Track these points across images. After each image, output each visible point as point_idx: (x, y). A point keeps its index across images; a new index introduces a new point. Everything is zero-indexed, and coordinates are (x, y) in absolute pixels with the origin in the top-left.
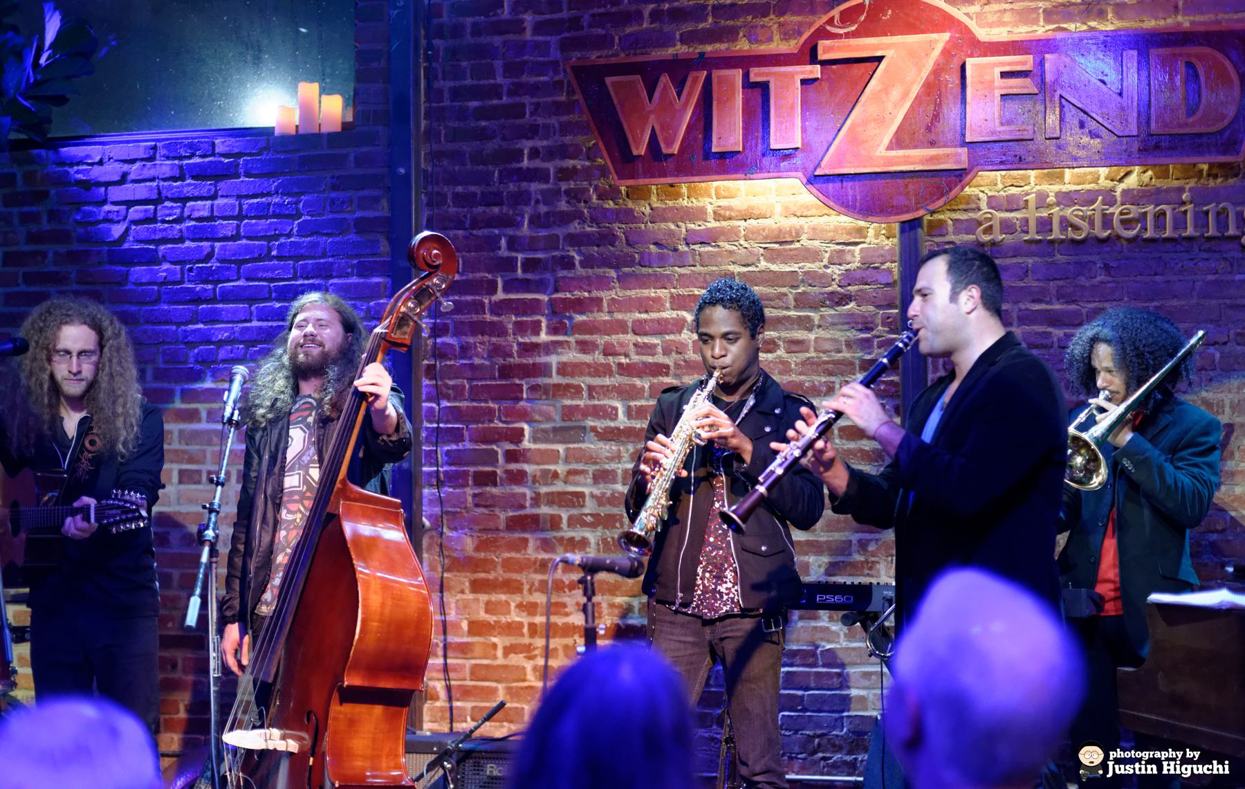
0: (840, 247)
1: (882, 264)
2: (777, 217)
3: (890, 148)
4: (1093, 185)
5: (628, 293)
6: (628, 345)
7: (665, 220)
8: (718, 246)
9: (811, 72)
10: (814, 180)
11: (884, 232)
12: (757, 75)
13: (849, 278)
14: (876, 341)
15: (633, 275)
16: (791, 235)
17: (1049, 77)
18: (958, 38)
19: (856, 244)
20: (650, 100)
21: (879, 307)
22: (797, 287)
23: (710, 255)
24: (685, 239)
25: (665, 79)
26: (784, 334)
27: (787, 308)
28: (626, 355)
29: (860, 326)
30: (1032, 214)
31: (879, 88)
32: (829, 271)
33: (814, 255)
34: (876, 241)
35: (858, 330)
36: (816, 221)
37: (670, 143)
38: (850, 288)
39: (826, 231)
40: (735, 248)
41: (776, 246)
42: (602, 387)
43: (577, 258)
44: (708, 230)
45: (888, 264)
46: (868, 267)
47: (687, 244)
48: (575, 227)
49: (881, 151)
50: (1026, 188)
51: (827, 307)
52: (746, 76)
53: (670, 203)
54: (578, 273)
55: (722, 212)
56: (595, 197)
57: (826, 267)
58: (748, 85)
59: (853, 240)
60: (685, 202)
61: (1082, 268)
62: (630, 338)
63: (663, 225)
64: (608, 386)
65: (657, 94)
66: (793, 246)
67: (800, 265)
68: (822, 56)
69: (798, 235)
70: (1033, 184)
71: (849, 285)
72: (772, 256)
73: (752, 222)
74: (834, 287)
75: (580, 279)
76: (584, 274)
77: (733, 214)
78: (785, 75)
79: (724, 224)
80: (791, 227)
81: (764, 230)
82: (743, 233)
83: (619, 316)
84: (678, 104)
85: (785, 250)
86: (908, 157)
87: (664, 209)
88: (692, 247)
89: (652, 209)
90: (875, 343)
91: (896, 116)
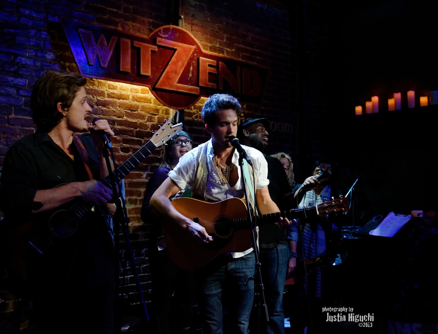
3: (178, 83)
8: (109, 108)
9: (155, 48)
10: (154, 90)
11: (164, 112)
12: (137, 44)
16: (135, 108)
17: (220, 70)
18: (197, 49)
19: (156, 115)
22: (136, 128)
23: (108, 111)
24: (96, 103)
26: (132, 146)
27: (133, 136)
31: (175, 60)
32: (147, 123)
33: (142, 117)
34: (162, 115)
36: (143, 104)
39: (147, 108)
40: (115, 110)
41: (129, 111)
44: (105, 101)
47: (97, 105)
49: (175, 83)
53: (91, 87)
55: (111, 95)
57: (146, 122)
58: (133, 47)
59: (155, 113)
60: (97, 87)
66: (135, 112)
67: (138, 120)
68: (159, 44)
72: (128, 115)
73: (121, 100)
74: (149, 130)
77: (115, 96)
79: (111, 99)
80: (135, 105)
81: (126, 104)
82: (118, 104)
85: (133, 113)
88: (100, 107)
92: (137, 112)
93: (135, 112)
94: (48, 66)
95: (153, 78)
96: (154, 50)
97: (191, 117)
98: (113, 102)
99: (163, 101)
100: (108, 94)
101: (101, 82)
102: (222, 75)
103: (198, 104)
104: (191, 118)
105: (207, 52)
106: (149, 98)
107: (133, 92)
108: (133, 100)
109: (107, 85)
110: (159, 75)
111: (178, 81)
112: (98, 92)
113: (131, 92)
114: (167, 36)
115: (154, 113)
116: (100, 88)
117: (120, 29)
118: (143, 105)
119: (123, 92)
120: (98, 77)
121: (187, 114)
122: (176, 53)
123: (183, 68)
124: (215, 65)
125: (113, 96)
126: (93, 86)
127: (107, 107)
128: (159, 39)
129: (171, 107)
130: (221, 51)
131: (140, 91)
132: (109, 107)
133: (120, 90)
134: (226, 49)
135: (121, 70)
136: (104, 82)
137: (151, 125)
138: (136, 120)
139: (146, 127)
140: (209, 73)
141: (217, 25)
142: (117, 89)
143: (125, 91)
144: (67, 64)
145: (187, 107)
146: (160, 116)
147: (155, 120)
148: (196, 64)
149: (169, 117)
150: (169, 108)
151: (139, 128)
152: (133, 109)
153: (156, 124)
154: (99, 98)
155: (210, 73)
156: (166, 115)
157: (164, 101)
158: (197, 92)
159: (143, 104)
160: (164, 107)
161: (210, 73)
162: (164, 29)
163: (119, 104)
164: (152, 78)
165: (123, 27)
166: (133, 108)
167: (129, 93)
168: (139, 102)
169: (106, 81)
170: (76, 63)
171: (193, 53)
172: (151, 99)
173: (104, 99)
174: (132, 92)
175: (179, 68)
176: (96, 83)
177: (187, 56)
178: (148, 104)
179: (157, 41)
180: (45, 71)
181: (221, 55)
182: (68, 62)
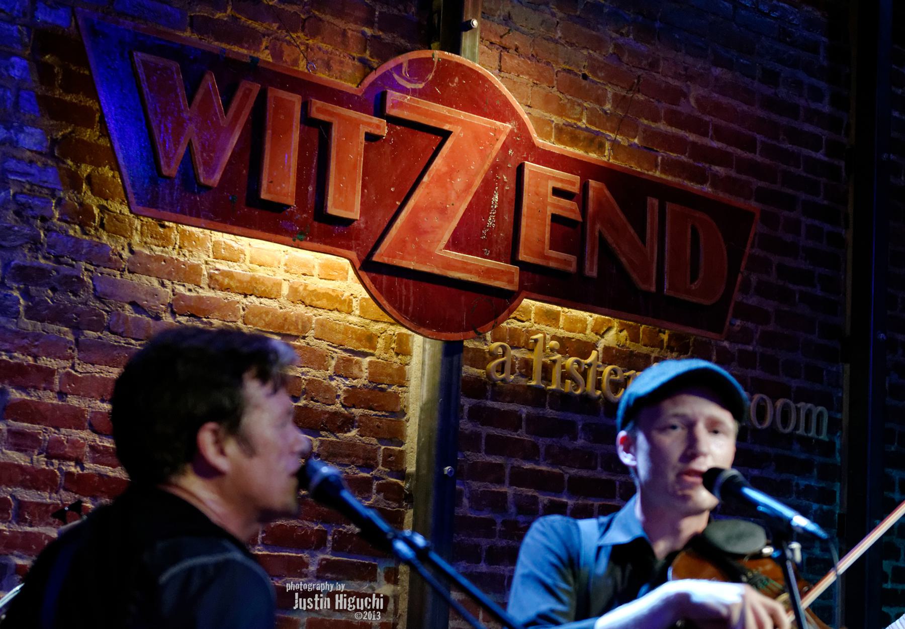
0: (346, 355)
1: (390, 385)
2: (282, 300)
3: (447, 247)
4: (581, 335)
5: (89, 368)
6: (83, 445)
7: (148, 272)
9: (378, 127)
11: (393, 345)
12: (320, 109)
13: (354, 397)
14: (375, 484)
15: (101, 345)
18: (517, 135)
19: (365, 355)
20: (191, 99)
21: (381, 440)
24: (170, 305)
25: (210, 80)
28: (79, 463)
29: (361, 462)
30: (537, 359)
31: (444, 169)
32: (334, 383)
34: (385, 356)
35: (358, 467)
36: (324, 315)
37: (210, 172)
38: (353, 410)
42: (39, 505)
43: (21, 301)
44: (200, 299)
45: (394, 388)
46: (375, 387)
47: (173, 314)
48: (23, 257)
49: (440, 250)
50: (527, 324)
51: (327, 431)
52: (305, 107)
53: (158, 250)
54: (23, 326)
55: (220, 278)
56: (57, 215)
58: (307, 121)
60: (175, 252)
61: (568, 428)
62: (85, 435)
63: (144, 278)
64: (48, 505)
65: (198, 97)
66: (297, 343)
67: (304, 369)
69: (305, 329)
70: (533, 321)
71: (354, 407)
73: (253, 299)
74: (337, 407)
75: (21, 334)
76: (30, 328)
78: (350, 119)
79: (220, 294)
80: (298, 317)
81: (267, 313)
82: (242, 313)
83: (73, 401)
84: (224, 122)
86: (466, 263)
87: (149, 257)
89: (132, 251)
90: (374, 487)
91: (458, 210)
92: (302, 341)
93: (297, 343)
94: (24, 174)
95: (366, 228)
96: (377, 132)
97: (484, 368)
98: (226, 304)
99: (395, 308)
100: (211, 276)
101: (191, 234)
102: (598, 226)
103: (507, 323)
104: (483, 371)
105: (547, 143)
106: (347, 294)
107: (292, 271)
108: (291, 299)
109: (210, 245)
110: (387, 219)
111: (449, 241)
112: (178, 269)
113: (287, 272)
114: (421, 86)
115: (359, 348)
116: (187, 254)
117: (265, 56)
118: (323, 320)
119: (261, 273)
120: (182, 217)
121: (470, 354)
122: (449, 144)
123: (470, 198)
124: (575, 189)
125: (228, 284)
126: (164, 247)
127: (205, 320)
128: (393, 96)
129: (422, 330)
130: (594, 141)
131: (316, 272)
132: (212, 321)
133: (251, 263)
134: (613, 135)
135: (264, 196)
136: (201, 235)
137: (345, 388)
138: (299, 369)
139: (329, 394)
140: (553, 216)
141: (585, 52)
142: (241, 260)
143: (269, 268)
144: (86, 170)
145: (472, 333)
146: (379, 359)
147: (362, 371)
148: (513, 185)
149: (407, 364)
150: (410, 332)
151: (305, 399)
152: (289, 330)
153: (364, 385)
154: (181, 289)
155: (555, 218)
156: (400, 357)
157: (399, 310)
158: (510, 282)
159: (324, 315)
160: (392, 327)
161: (555, 218)
162: (411, 62)
163: (246, 312)
164: (362, 226)
165: (277, 54)
166: (292, 328)
167: (280, 275)
168: (312, 308)
169: (207, 232)
170: (116, 167)
171: (505, 147)
172: (352, 297)
173: (198, 293)
174: (291, 274)
175: (453, 196)
176: (175, 236)
177: (483, 155)
178: (343, 316)
179: (389, 104)
180: (12, 192)
181: (593, 156)
182: (91, 163)
